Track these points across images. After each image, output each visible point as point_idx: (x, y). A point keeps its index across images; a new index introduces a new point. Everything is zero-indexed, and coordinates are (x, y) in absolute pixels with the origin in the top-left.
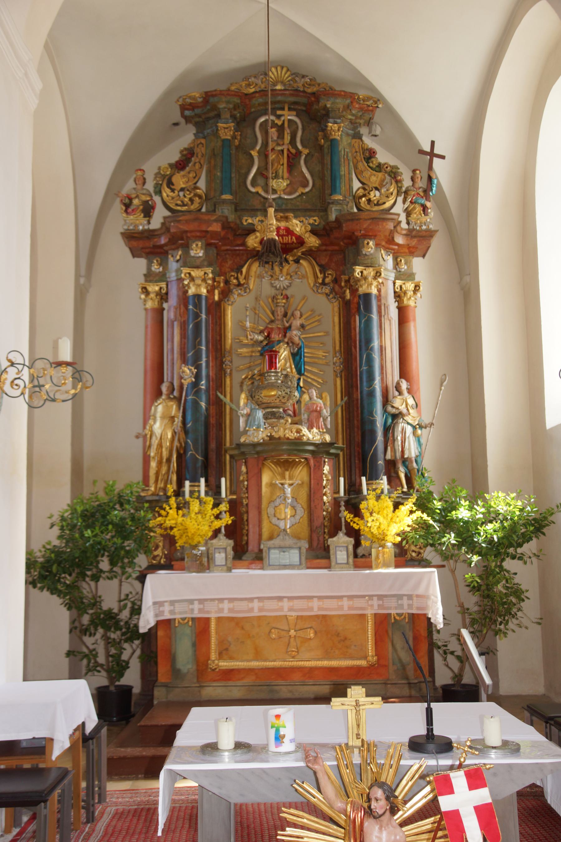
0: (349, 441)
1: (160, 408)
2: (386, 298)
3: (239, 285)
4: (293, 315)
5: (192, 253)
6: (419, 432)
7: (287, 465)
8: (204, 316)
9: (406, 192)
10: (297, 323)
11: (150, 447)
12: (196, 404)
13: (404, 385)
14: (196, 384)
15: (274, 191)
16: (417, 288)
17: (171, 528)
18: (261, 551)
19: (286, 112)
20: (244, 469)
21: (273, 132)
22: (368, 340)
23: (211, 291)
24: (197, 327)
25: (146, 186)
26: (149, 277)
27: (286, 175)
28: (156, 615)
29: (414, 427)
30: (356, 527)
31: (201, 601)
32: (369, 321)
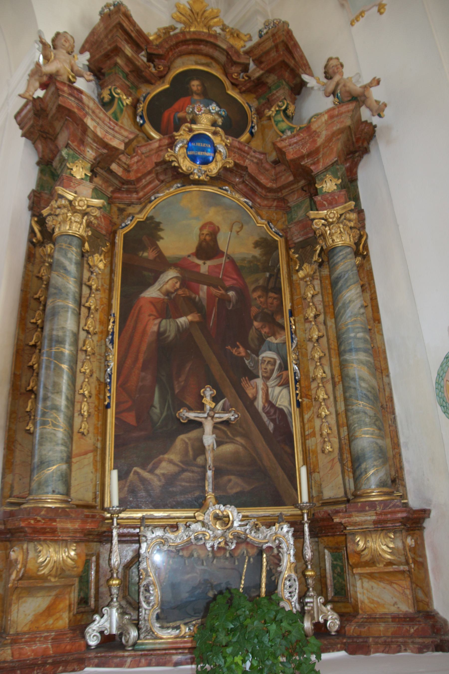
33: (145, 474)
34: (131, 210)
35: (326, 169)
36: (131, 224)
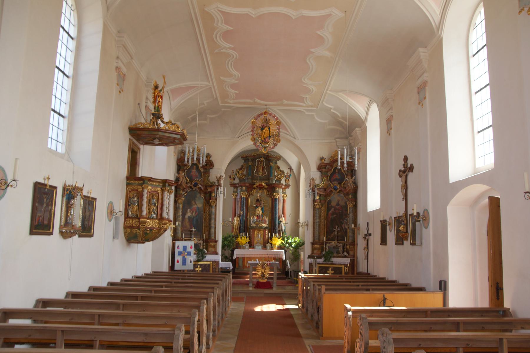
0: (272, 226)
1: (236, 219)
2: (280, 198)
3: (251, 194)
4: (262, 201)
5: (243, 189)
6: (285, 225)
7: (260, 230)
8: (245, 201)
9: (285, 176)
10: (263, 203)
11: (234, 226)
12: (243, 218)
13: (282, 216)
14: (243, 215)
15: (259, 175)
16: (286, 196)
17: (239, 242)
18: (254, 246)
19: (262, 158)
20: (251, 231)
21: (259, 162)
22: (276, 207)
23: (246, 196)
24: (243, 203)
25: (234, 173)
26: (234, 192)
27: (262, 172)
28: (236, 256)
29: (284, 224)
30: (271, 243)
31: (244, 254)
32: (276, 204)
33: (330, 237)
34: (328, 198)
35: (350, 194)
36: (327, 201)
